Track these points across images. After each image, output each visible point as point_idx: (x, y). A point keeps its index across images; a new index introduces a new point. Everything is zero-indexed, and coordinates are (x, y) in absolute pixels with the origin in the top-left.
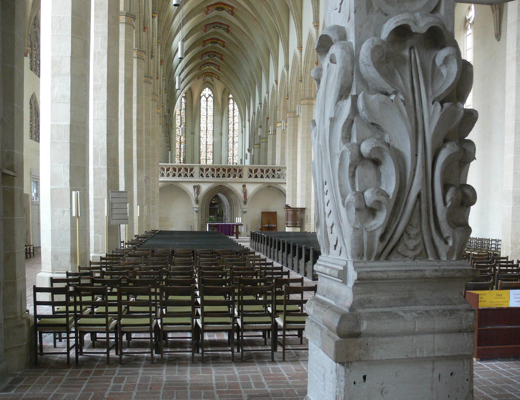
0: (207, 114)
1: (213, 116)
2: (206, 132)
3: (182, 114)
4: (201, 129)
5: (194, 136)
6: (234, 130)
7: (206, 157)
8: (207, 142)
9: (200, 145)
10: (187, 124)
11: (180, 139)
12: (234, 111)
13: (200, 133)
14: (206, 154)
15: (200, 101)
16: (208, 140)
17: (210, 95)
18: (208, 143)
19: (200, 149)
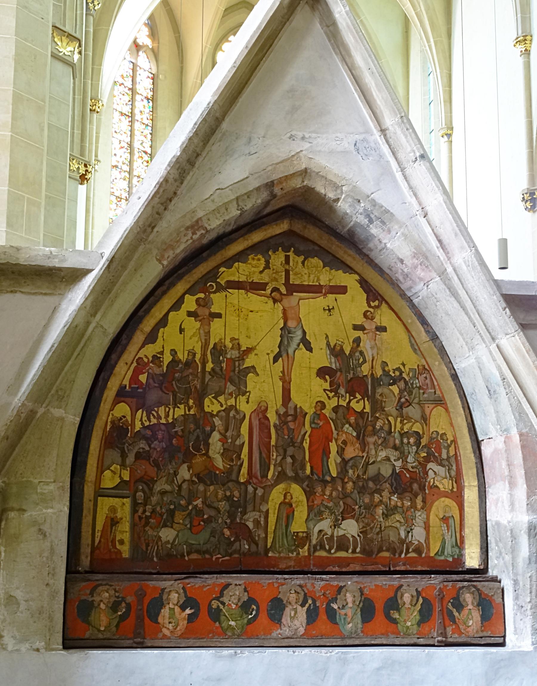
3: (138, 117)
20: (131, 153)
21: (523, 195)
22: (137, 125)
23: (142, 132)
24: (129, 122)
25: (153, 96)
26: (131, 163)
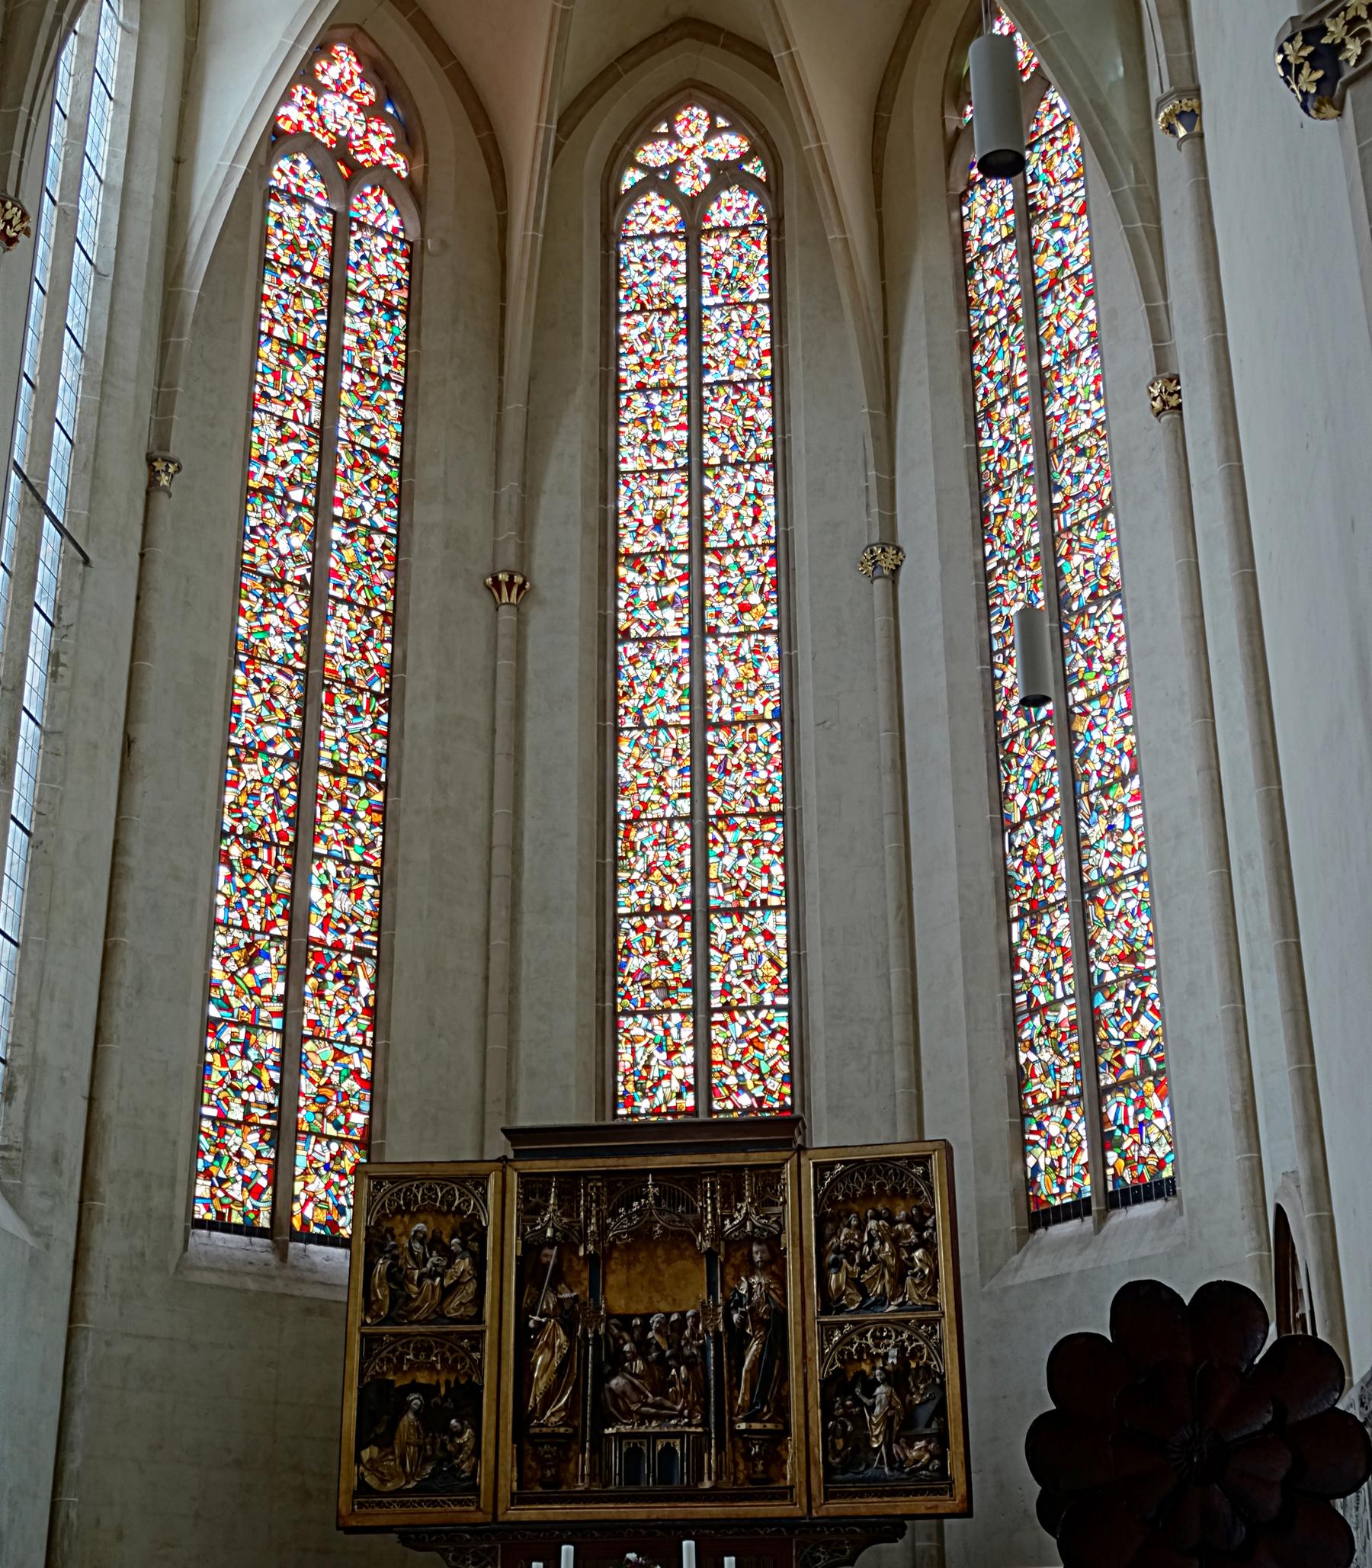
0: (697, 368)
1: (778, 383)
2: (693, 576)
4: (628, 543)
5: (521, 622)
6: (1047, 448)
7: (700, 876)
8: (699, 693)
9: (608, 735)
10: (429, 474)
11: (311, 636)
12: (1041, 230)
13: (606, 584)
14: (700, 847)
15: (610, 237)
16: (711, 660)
17: (725, 174)
18: (715, 699)
19: (608, 788)
20: (326, 455)
21: (1281, 50)
22: (348, 377)
23: (368, 398)
24: (317, 368)
25: (408, 300)
26: (322, 484)
